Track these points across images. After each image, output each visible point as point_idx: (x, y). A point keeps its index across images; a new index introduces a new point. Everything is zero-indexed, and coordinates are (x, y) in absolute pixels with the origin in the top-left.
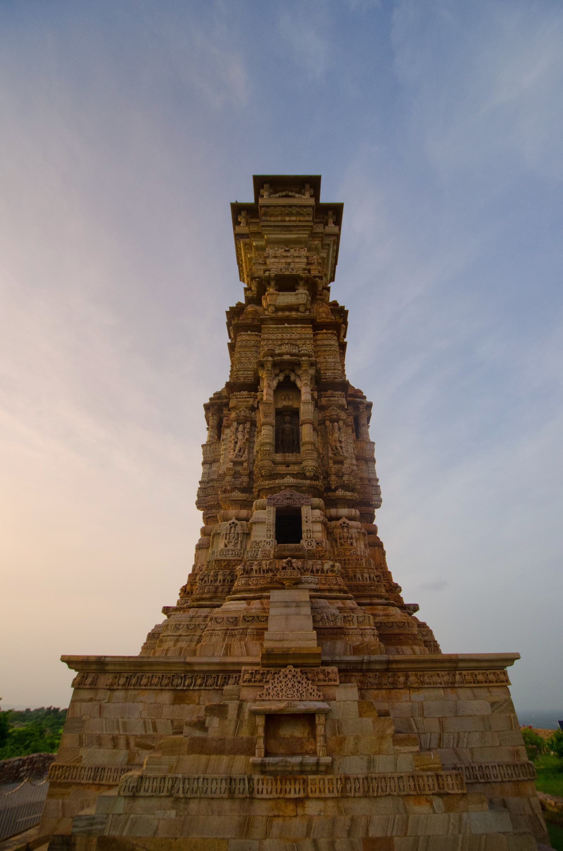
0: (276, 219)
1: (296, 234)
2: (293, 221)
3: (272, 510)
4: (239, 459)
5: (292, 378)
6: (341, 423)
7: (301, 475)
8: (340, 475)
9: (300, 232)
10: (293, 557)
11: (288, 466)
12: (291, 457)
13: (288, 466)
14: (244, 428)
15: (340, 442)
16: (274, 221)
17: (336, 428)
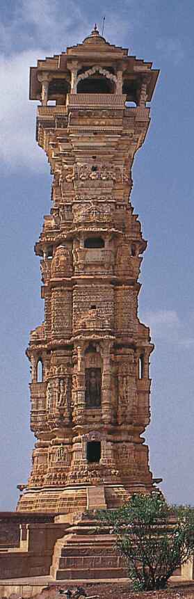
0: (85, 123)
1: (105, 142)
2: (103, 125)
3: (85, 443)
4: (62, 407)
5: (98, 351)
6: (128, 377)
7: (102, 422)
8: (124, 416)
9: (109, 140)
10: (97, 470)
11: (94, 416)
12: (95, 411)
13: (94, 416)
14: (64, 382)
15: (127, 392)
16: (83, 125)
17: (125, 382)
